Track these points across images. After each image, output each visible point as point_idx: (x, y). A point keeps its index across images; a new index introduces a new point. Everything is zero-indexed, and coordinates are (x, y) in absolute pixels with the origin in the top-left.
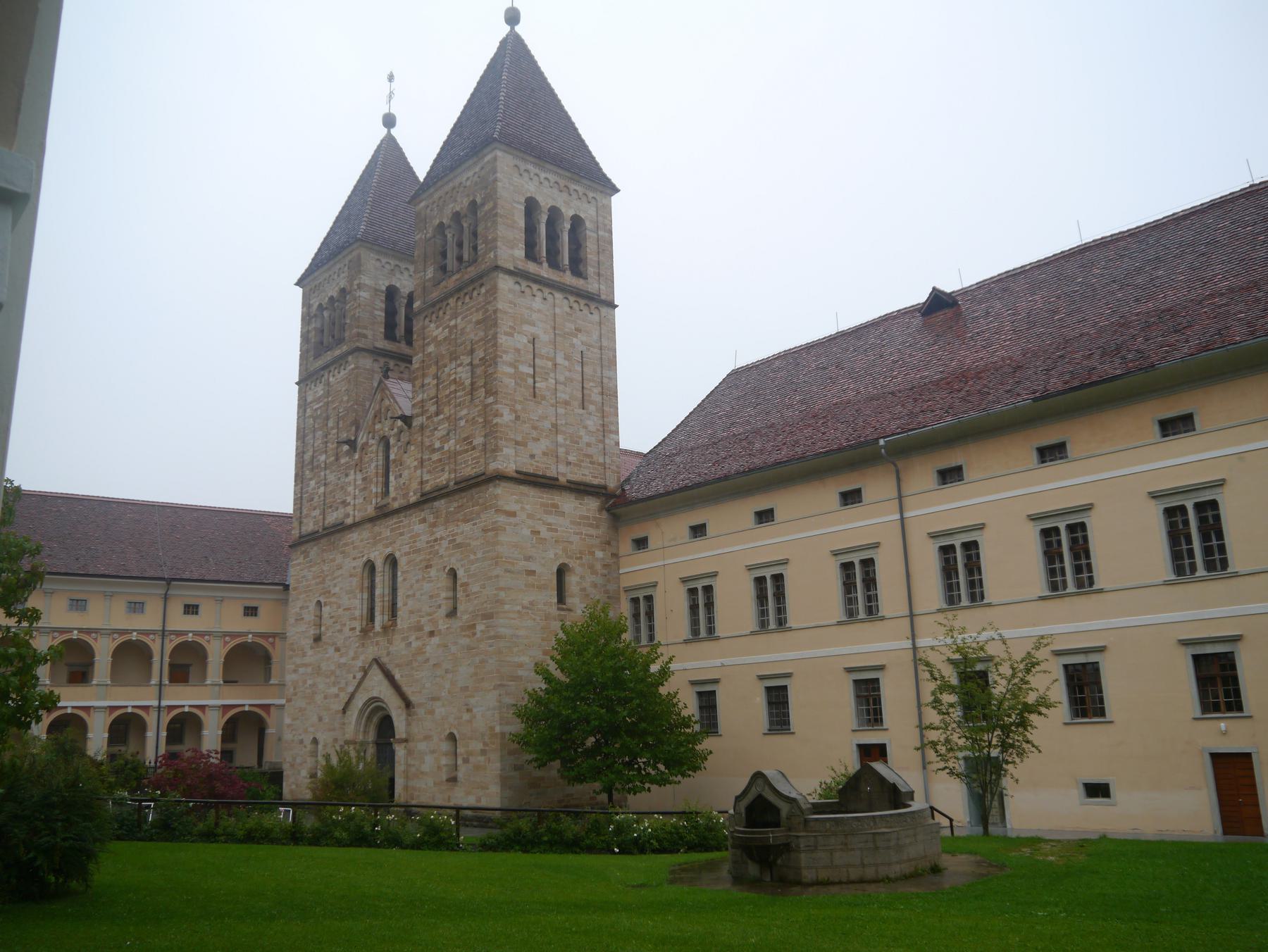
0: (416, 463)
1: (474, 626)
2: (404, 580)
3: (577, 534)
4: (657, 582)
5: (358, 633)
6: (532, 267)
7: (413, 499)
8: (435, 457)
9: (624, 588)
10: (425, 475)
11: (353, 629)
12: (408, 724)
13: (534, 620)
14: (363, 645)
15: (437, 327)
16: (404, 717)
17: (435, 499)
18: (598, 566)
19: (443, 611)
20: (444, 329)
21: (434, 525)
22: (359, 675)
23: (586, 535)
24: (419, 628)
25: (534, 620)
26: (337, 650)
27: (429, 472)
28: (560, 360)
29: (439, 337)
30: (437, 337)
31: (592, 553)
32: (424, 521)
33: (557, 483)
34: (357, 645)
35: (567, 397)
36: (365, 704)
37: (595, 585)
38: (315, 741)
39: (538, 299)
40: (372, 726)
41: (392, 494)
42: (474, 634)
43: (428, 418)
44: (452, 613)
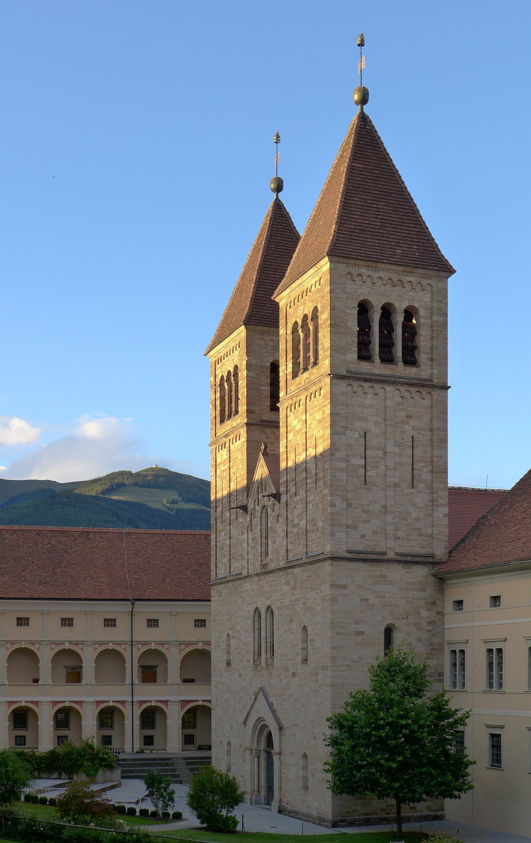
0: (283, 534)
1: (317, 674)
2: (278, 628)
3: (404, 598)
4: (468, 640)
5: (252, 665)
6: (365, 367)
7: (282, 564)
8: (295, 531)
9: (447, 641)
10: (289, 545)
11: (249, 661)
12: (280, 742)
13: (363, 671)
14: (255, 674)
15: (295, 419)
16: (278, 735)
17: (293, 567)
18: (424, 624)
19: (299, 659)
20: (299, 421)
21: (294, 588)
22: (253, 698)
23: (412, 598)
24: (287, 669)
25: (363, 671)
26: (240, 675)
27: (291, 543)
28: (390, 448)
29: (296, 427)
30: (295, 426)
31: (418, 613)
32: (288, 583)
33: (386, 557)
34: (252, 674)
35: (397, 480)
36: (256, 721)
37: (420, 640)
38: (229, 744)
39: (370, 396)
40: (263, 738)
41: (270, 556)
42: (317, 681)
43: (291, 497)
44: (305, 661)
